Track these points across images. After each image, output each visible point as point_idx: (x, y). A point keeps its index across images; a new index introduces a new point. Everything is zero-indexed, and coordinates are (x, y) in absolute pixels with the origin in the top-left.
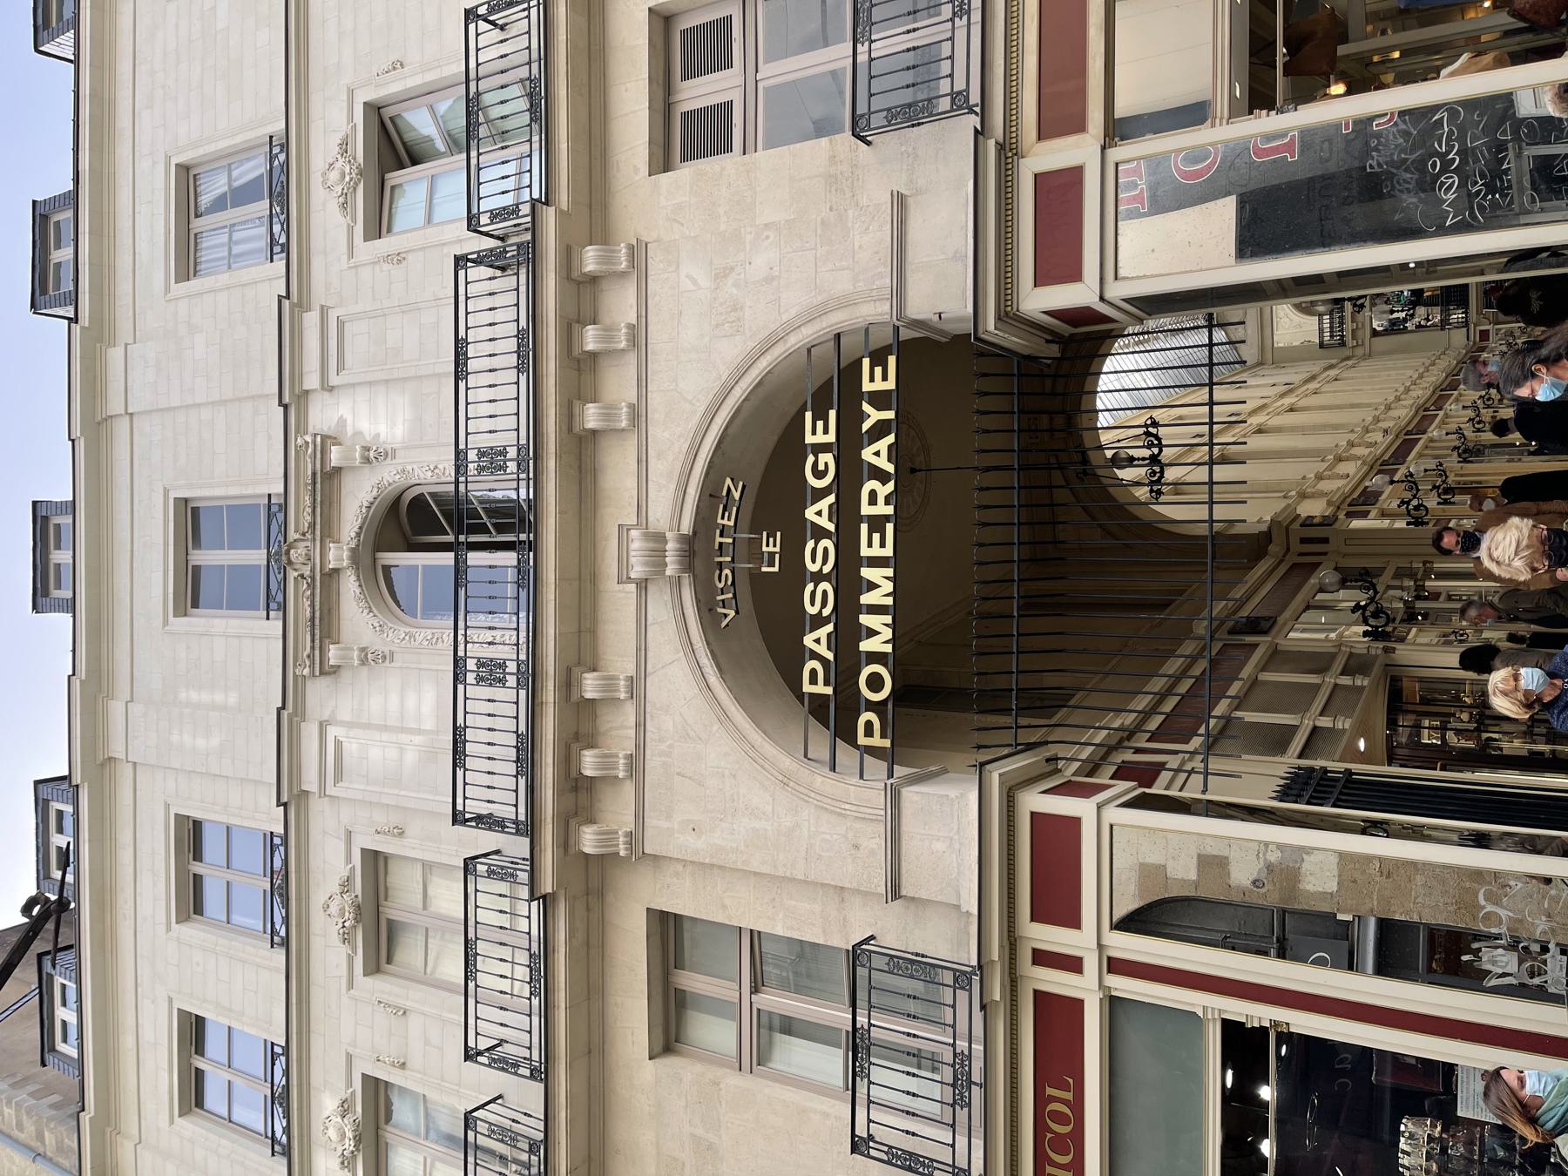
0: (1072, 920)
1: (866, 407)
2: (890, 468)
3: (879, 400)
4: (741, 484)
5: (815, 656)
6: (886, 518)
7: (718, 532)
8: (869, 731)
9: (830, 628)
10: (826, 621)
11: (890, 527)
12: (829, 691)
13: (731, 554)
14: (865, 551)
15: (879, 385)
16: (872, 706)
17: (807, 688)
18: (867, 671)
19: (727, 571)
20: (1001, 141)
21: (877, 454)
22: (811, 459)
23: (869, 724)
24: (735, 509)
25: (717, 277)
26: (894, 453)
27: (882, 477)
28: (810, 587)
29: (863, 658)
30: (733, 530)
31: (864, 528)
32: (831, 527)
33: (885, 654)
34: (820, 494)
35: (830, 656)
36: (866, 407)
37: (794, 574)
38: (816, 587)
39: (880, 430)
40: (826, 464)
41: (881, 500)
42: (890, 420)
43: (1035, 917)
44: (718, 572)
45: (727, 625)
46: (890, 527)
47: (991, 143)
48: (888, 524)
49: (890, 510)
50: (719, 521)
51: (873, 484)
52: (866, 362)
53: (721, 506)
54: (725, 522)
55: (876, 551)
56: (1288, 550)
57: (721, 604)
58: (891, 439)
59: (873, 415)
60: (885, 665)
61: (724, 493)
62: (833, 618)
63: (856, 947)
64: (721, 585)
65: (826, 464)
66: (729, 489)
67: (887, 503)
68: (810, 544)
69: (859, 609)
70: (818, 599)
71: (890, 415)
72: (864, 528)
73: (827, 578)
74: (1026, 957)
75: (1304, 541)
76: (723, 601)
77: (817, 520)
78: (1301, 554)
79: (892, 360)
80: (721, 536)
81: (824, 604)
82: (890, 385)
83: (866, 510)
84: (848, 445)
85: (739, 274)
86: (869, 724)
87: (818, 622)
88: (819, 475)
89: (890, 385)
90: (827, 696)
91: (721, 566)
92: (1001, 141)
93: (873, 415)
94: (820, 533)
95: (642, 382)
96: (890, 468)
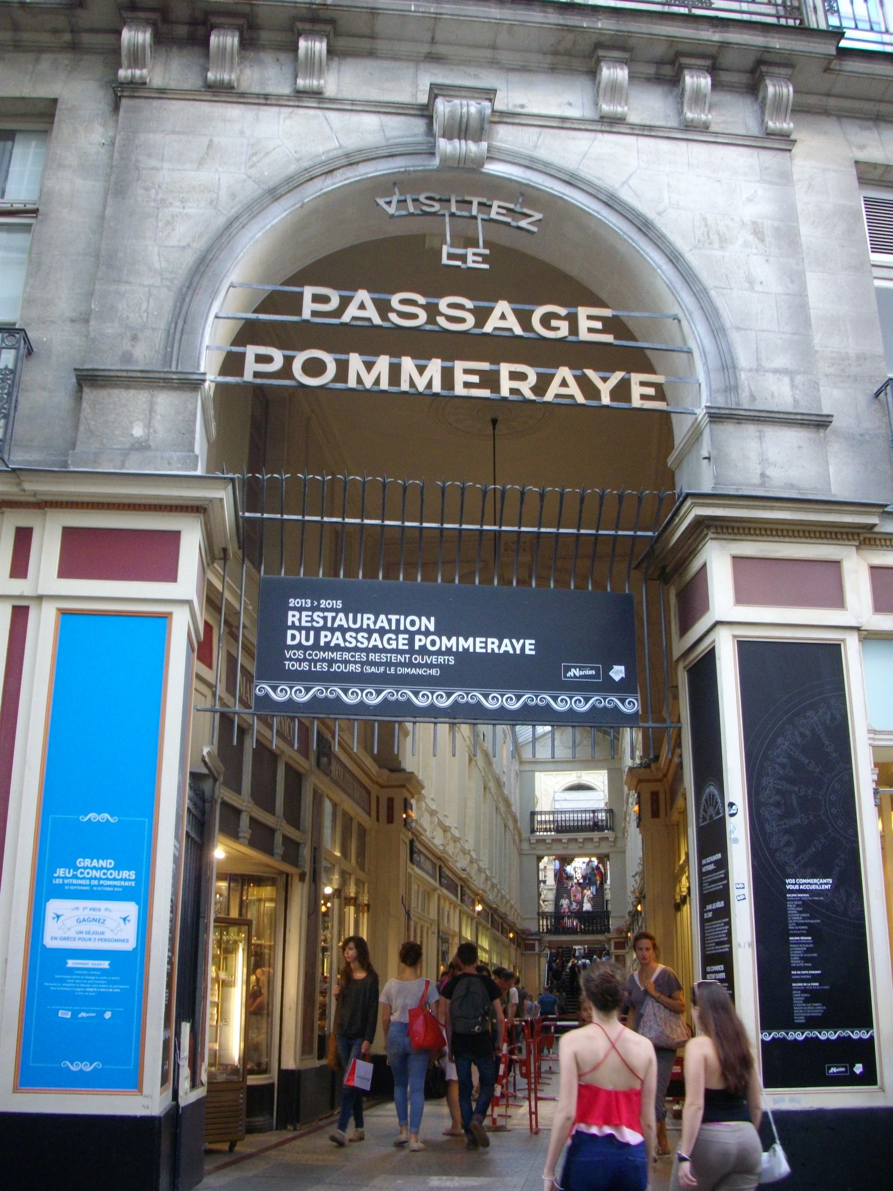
0: (67, 570)
2: (549, 397)
3: (622, 391)
4: (534, 229)
5: (345, 302)
6: (496, 388)
7: (484, 200)
9: (377, 320)
10: (384, 317)
11: (485, 393)
12: (306, 314)
13: (458, 213)
14: (459, 366)
16: (289, 361)
17: (308, 292)
18: (328, 358)
19: (437, 207)
20: (876, 529)
22: (563, 311)
23: (269, 359)
25: (754, 223)
28: (421, 300)
29: (343, 357)
30: (485, 217)
31: (485, 366)
32: (488, 328)
33: (345, 380)
34: (524, 319)
35: (346, 318)
40: (557, 329)
41: (516, 384)
42: (599, 399)
43: (68, 533)
44: (437, 197)
45: (378, 204)
46: (485, 393)
47: (873, 520)
48: (489, 391)
49: (505, 392)
50: (496, 204)
51: (532, 379)
53: (511, 206)
54: (495, 209)
55: (460, 378)
56: (382, 787)
57: (402, 198)
58: (580, 399)
60: (335, 380)
62: (386, 324)
63: (23, 334)
64: (422, 198)
65: (557, 329)
66: (529, 216)
68: (469, 304)
69: (396, 352)
72: (485, 366)
73: (431, 320)
74: (23, 519)
75: (391, 801)
76: (405, 201)
77: (496, 313)
78: (378, 798)
80: (480, 204)
83: (505, 369)
85: (756, 248)
86: (269, 359)
88: (546, 320)
89: (636, 403)
92: (876, 529)
94: (482, 316)
95: (646, 130)
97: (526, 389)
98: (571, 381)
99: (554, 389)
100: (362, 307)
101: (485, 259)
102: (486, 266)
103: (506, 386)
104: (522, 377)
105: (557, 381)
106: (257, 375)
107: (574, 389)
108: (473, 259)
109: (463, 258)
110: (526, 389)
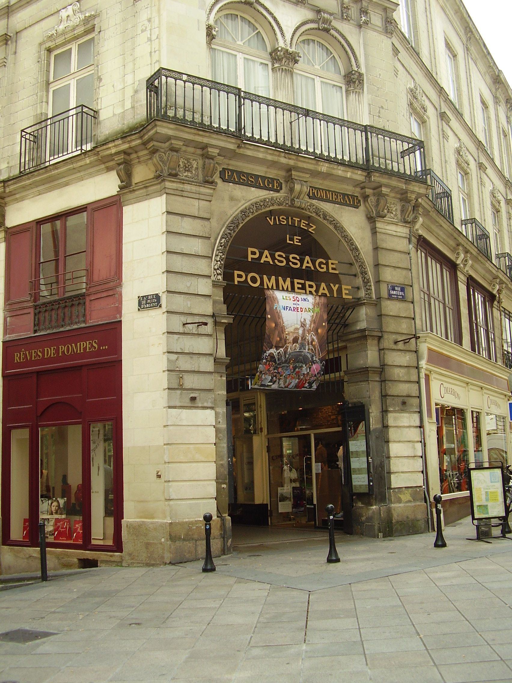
1: (337, 286)
4: (314, 232)
10: (273, 262)
12: (250, 260)
14: (296, 281)
24: (306, 228)
31: (303, 281)
35: (262, 261)
36: (337, 286)
37: (289, 249)
38: (284, 258)
39: (331, 290)
41: (311, 289)
53: (307, 223)
61: (311, 224)
72: (303, 281)
73: (287, 263)
82: (344, 296)
83: (308, 283)
87: (273, 258)
90: (260, 261)
91: (287, 219)
101: (300, 241)
102: (300, 244)
105: (321, 288)
108: (296, 241)
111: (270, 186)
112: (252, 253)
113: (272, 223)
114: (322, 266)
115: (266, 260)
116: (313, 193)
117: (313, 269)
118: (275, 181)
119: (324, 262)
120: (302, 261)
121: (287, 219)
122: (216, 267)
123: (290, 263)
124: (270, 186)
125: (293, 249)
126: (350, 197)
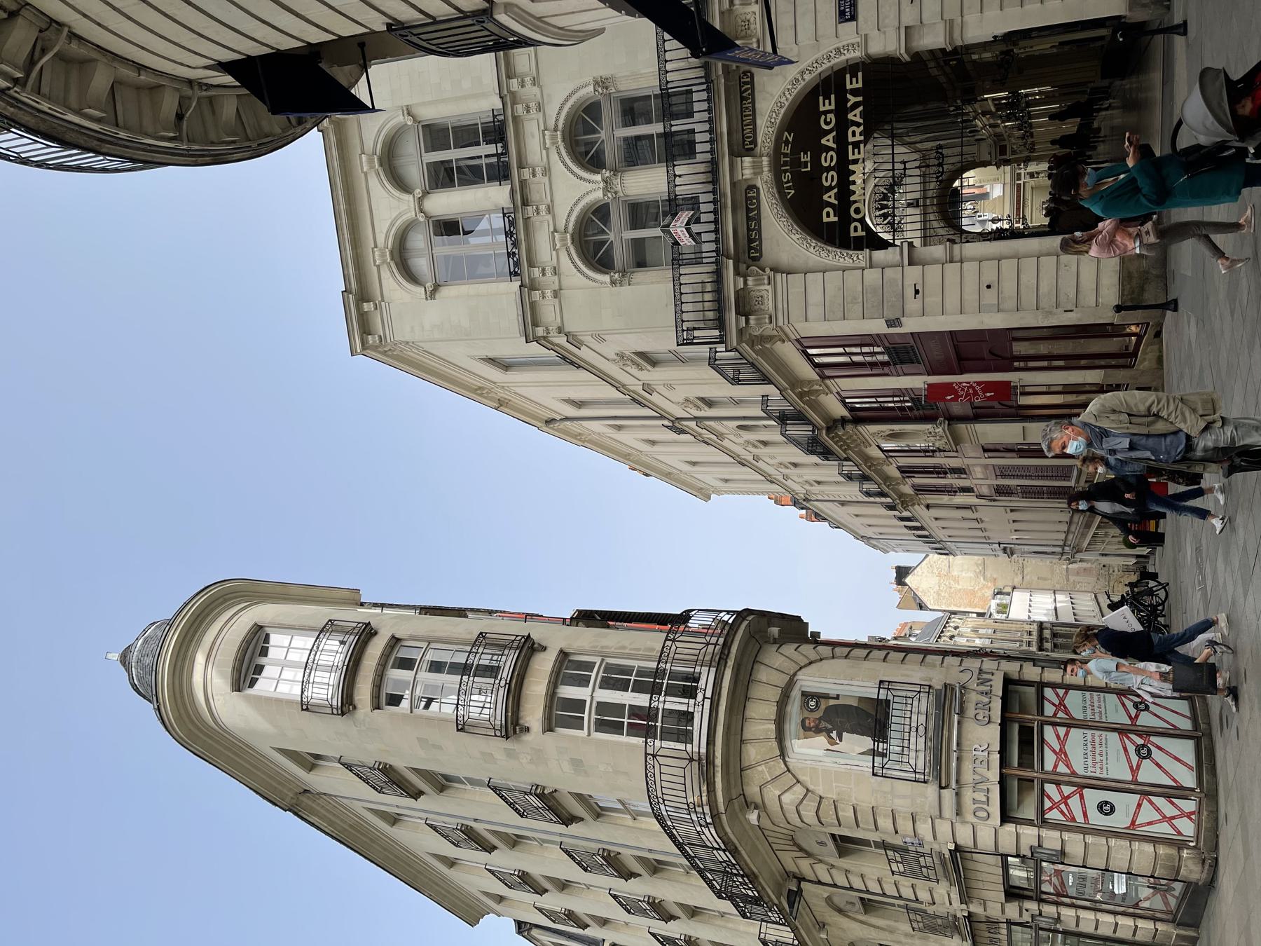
1: (849, 96)
2: (861, 121)
3: (855, 92)
5: (830, 205)
6: (860, 142)
8: (856, 229)
10: (834, 188)
12: (836, 219)
15: (855, 86)
21: (855, 116)
26: (862, 115)
27: (858, 125)
31: (850, 147)
35: (836, 202)
36: (849, 96)
37: (819, 169)
41: (857, 134)
51: (854, 128)
52: (848, 76)
54: (786, 151)
58: (861, 108)
59: (852, 99)
64: (785, 181)
67: (860, 135)
70: (829, 179)
71: (860, 99)
72: (850, 147)
79: (860, 74)
81: (832, 181)
82: (860, 85)
83: (851, 139)
84: (841, 111)
87: (830, 188)
89: (860, 85)
91: (786, 171)
93: (852, 99)
96: (861, 121)
97: (858, 130)
98: (854, 113)
99: (858, 119)
100: (830, 197)
101: (805, 153)
103: (859, 138)
104: (854, 133)
106: (862, 231)
107: (857, 111)
108: (806, 158)
109: (806, 163)
110: (858, 130)
111: (755, 201)
112: (829, 217)
113: (793, 192)
114: (828, 120)
115: (833, 197)
116: (751, 143)
117: (834, 133)
118: (749, 195)
119: (823, 117)
120: (828, 149)
121: (786, 171)
122: (851, 261)
123: (832, 164)
124: (755, 201)
125: (816, 160)
126: (743, 89)
